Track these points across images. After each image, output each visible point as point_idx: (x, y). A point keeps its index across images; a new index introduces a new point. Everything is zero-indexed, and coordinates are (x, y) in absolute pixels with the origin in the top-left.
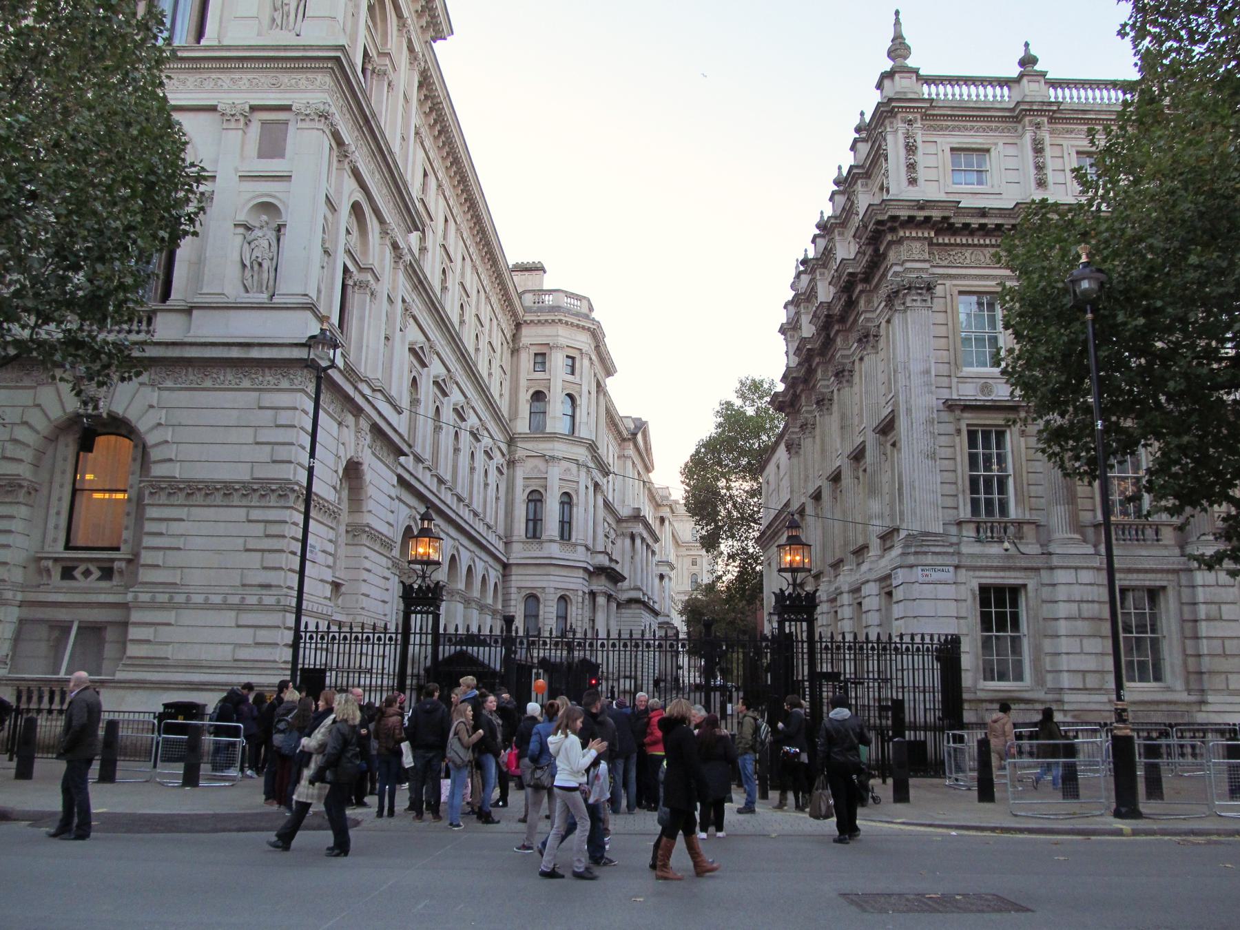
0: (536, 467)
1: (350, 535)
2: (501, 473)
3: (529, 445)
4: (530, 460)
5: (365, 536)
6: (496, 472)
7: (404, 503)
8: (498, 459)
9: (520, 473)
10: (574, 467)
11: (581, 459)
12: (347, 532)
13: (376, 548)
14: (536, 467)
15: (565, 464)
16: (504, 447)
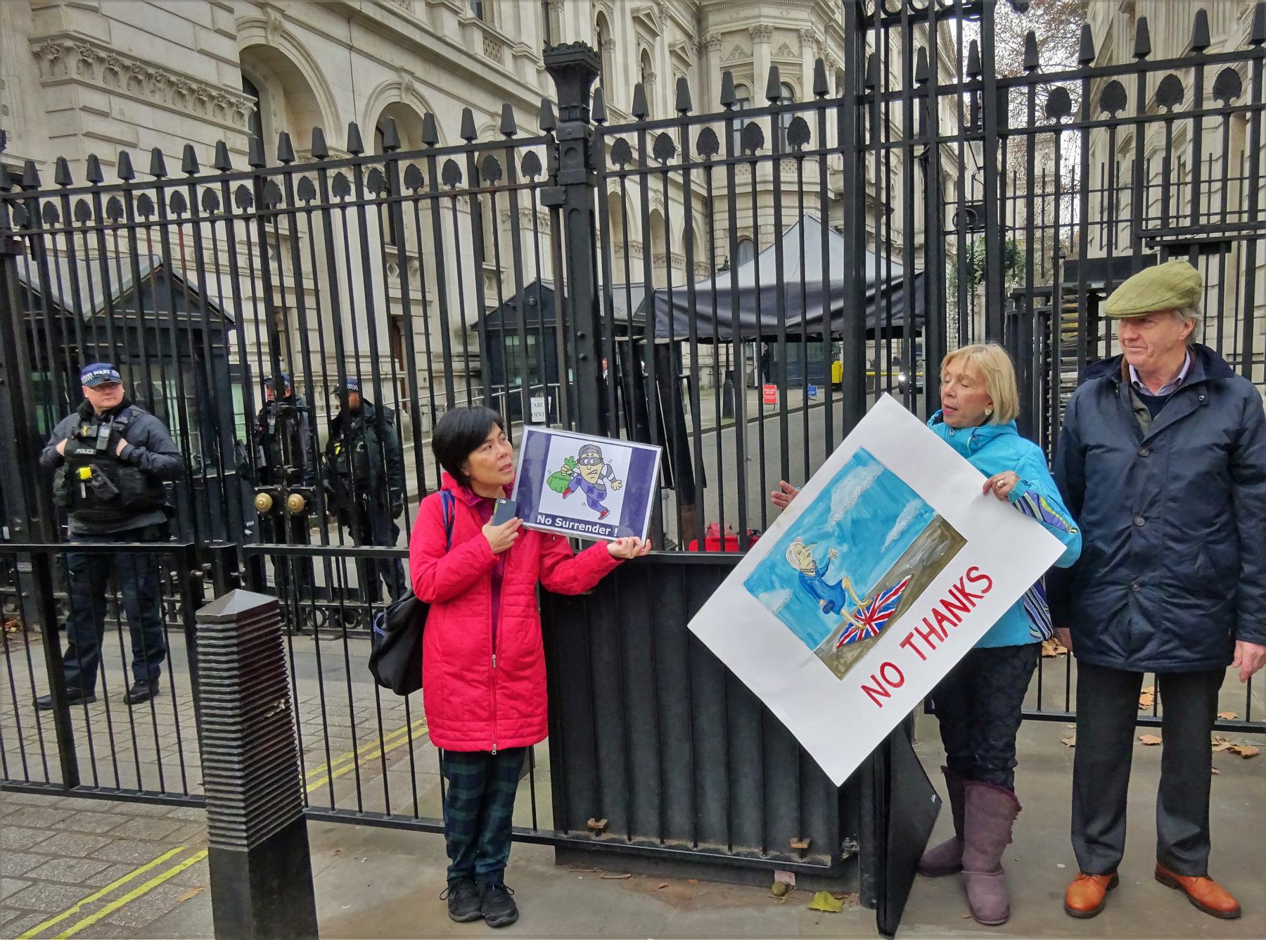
0: (737, 48)
1: (45, 65)
2: (687, 65)
3: (726, 16)
4: (728, 39)
5: (72, 62)
6: (669, 60)
7: (360, 52)
8: (670, 35)
9: (716, 62)
10: (792, 41)
11: (804, 26)
12: (37, 56)
13: (157, 99)
14: (737, 48)
15: (779, 38)
16: (687, 22)
